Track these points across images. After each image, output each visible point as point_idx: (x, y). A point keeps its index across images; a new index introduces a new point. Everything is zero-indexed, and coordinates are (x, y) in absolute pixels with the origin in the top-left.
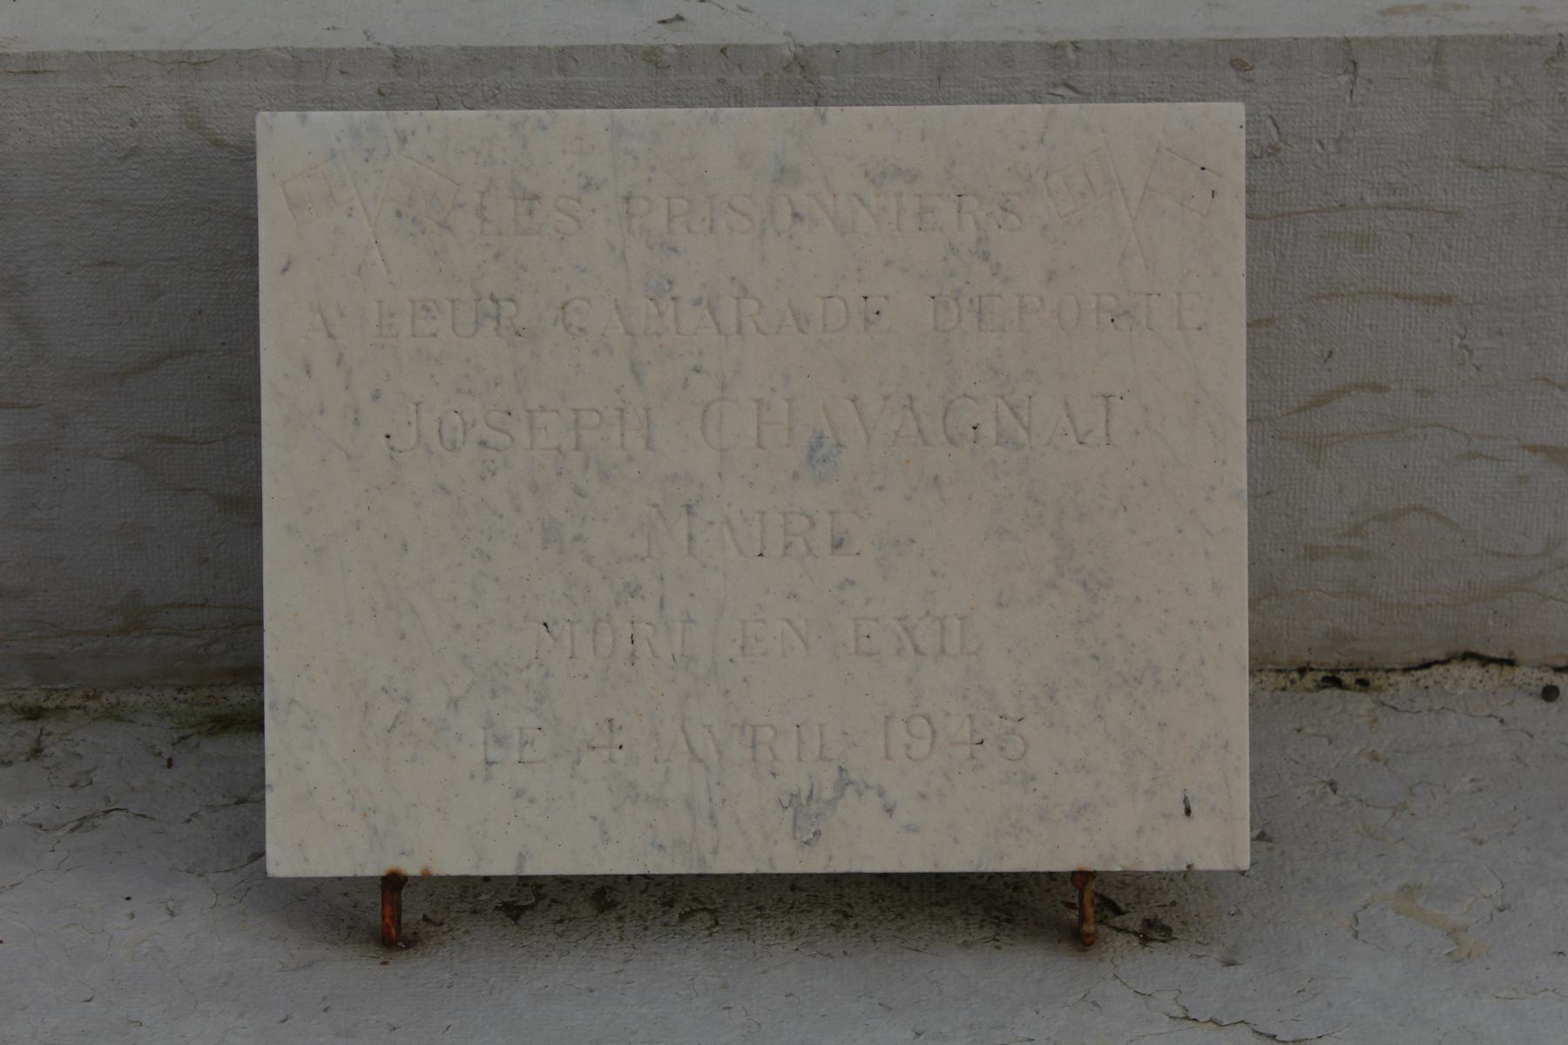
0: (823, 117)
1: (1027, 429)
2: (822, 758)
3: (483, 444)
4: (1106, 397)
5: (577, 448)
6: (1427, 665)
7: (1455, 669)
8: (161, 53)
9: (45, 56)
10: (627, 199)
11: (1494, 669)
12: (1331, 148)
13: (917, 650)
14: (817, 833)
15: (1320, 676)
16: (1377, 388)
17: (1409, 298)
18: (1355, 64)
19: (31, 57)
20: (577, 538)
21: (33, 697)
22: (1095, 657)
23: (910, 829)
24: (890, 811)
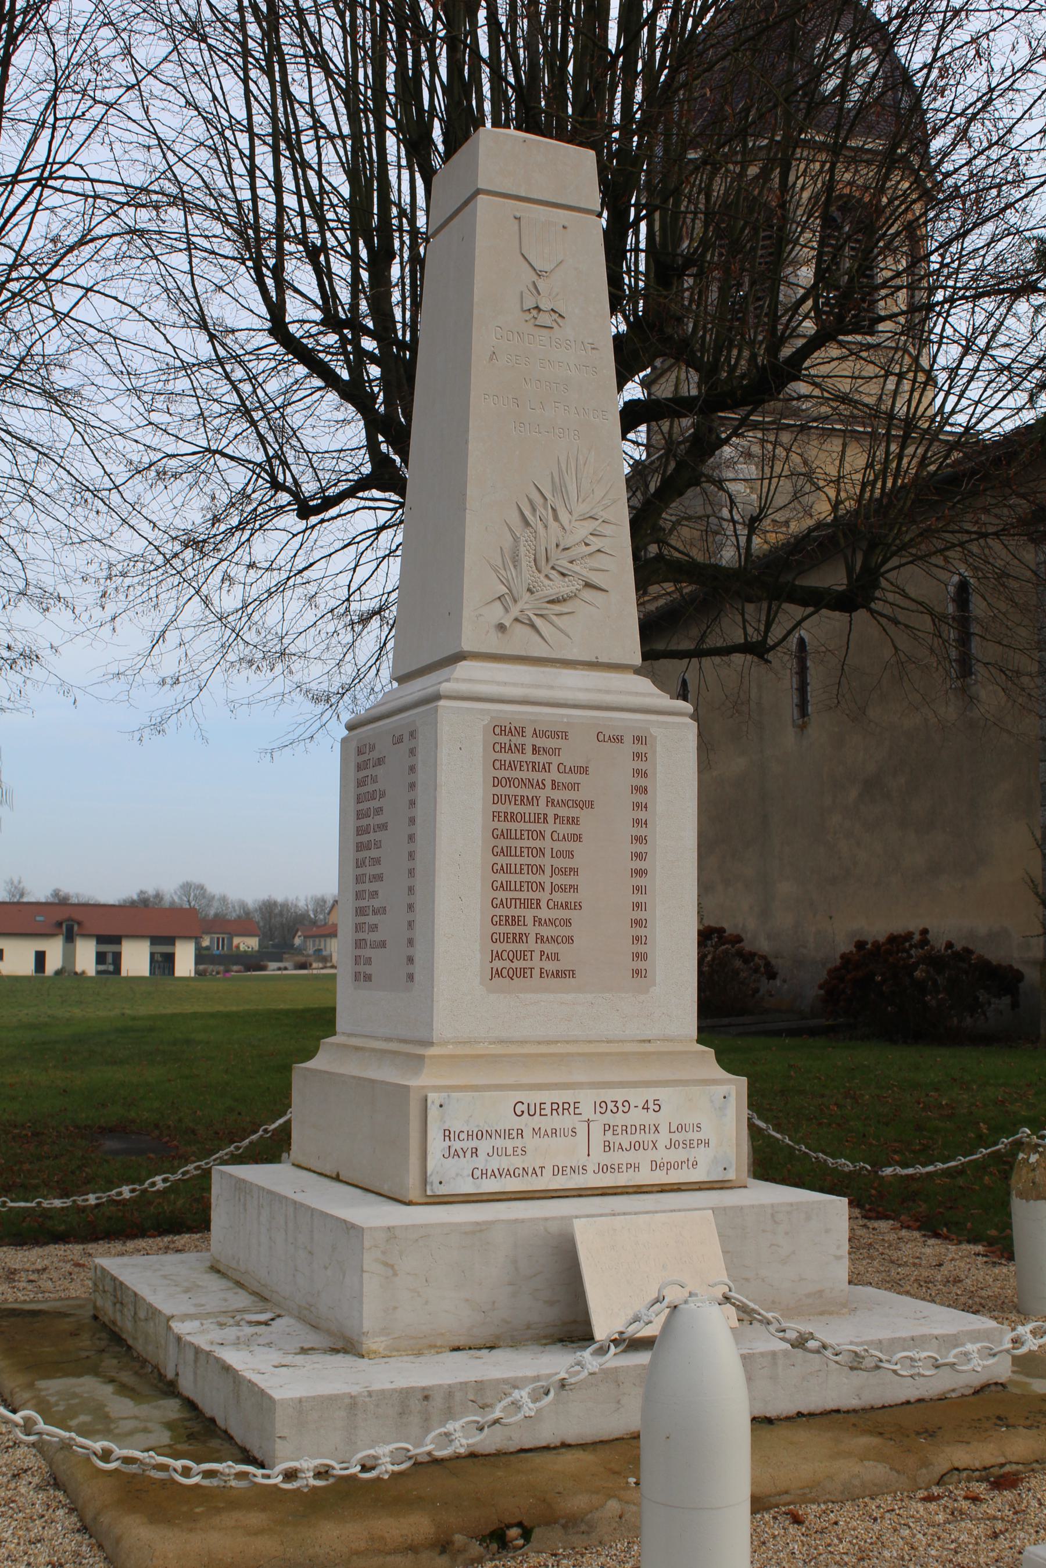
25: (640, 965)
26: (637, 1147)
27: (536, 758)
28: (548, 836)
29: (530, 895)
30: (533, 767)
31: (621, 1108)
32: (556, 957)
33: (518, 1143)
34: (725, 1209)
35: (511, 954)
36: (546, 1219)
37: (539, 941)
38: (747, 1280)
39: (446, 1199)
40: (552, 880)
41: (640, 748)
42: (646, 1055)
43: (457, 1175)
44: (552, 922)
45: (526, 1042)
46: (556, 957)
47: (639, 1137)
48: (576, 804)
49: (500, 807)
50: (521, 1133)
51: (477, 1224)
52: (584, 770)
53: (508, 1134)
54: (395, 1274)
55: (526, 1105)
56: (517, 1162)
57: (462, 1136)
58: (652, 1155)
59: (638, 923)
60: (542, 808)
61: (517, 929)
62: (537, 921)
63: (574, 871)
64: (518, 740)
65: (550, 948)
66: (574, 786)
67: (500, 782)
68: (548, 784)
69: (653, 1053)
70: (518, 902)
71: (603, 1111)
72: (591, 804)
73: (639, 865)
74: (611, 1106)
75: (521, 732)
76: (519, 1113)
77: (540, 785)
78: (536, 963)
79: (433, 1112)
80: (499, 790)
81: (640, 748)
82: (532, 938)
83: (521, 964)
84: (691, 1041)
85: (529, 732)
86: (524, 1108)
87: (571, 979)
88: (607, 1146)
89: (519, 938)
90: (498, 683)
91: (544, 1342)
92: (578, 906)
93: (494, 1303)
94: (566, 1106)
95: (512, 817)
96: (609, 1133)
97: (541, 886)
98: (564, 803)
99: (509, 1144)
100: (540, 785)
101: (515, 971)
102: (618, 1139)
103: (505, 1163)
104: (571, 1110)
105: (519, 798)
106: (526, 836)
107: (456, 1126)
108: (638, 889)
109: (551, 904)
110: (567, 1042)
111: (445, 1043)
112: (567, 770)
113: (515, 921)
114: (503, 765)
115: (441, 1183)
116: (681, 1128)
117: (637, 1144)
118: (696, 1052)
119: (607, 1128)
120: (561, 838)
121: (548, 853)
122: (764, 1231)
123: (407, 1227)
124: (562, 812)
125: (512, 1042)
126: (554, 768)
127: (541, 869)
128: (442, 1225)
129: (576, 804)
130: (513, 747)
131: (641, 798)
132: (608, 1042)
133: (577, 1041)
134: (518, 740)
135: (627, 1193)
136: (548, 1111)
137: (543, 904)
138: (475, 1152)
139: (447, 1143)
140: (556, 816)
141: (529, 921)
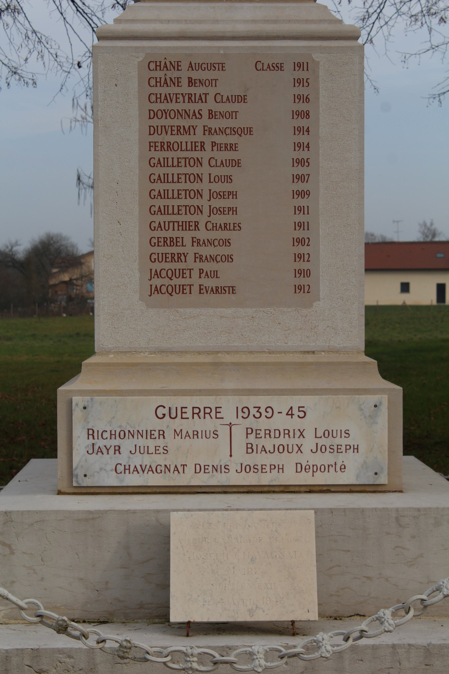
0: (253, 512)
1: (283, 556)
2: (254, 604)
3: (203, 558)
4: (295, 552)
5: (217, 559)
6: (351, 616)
7: (356, 617)
8: (153, 510)
9: (136, 510)
10: (224, 524)
11: (362, 617)
12: (330, 526)
13: (268, 588)
14: (253, 615)
15: (334, 618)
16: (339, 566)
17: (343, 551)
18: (332, 512)
19: (134, 510)
20: (217, 572)
21: (123, 620)
22: (294, 589)
23: (267, 614)
24: (264, 612)
25: (303, 281)
26: (281, 450)
27: (192, 90)
28: (205, 162)
29: (188, 218)
30: (189, 98)
31: (264, 413)
32: (215, 275)
33: (160, 442)
34: (345, 510)
35: (170, 272)
36: (158, 511)
37: (198, 260)
38: (369, 578)
39: (92, 490)
40: (210, 203)
41: (302, 74)
42: (302, 365)
43: (101, 469)
44: (211, 243)
45: (186, 352)
46: (215, 275)
47: (283, 441)
48: (234, 131)
49: (156, 138)
50: (162, 434)
51: (90, 512)
52: (243, 99)
53: (150, 434)
54: (12, 553)
55: (167, 409)
56: (160, 460)
57: (105, 435)
58: (295, 457)
59: (300, 241)
60: (199, 137)
61: (175, 250)
62: (196, 242)
63: (233, 194)
64: (173, 74)
65: (208, 267)
66: (232, 115)
67: (156, 114)
68: (205, 113)
69: (311, 364)
70: (176, 225)
71: (245, 416)
72: (250, 131)
73: (301, 186)
74: (253, 411)
75: (177, 66)
76: (161, 416)
77: (197, 115)
78: (195, 280)
79: (77, 414)
80: (156, 122)
81: (302, 74)
82: (190, 258)
83: (181, 281)
84: (358, 353)
85: (185, 65)
86: (166, 411)
87: (231, 295)
88: (250, 448)
89: (178, 257)
90: (161, 21)
91: (157, 620)
92: (237, 227)
93: (107, 583)
94: (208, 410)
95: (169, 146)
96: (252, 438)
97: (199, 209)
98: (222, 131)
99: (151, 444)
100: (197, 115)
101: (174, 288)
102: (261, 442)
103: (147, 460)
104: (213, 414)
105: (175, 129)
106: (183, 163)
107: (99, 426)
108: (300, 209)
109: (210, 226)
110: (228, 353)
111: (109, 352)
112: (224, 100)
113: (173, 242)
114: (158, 99)
115: (85, 476)
116: (328, 434)
117: (281, 448)
118: (365, 363)
119: (249, 431)
120: (219, 164)
121: (206, 178)
122: (388, 534)
123: (23, 513)
124: (220, 139)
125: (172, 352)
126: (210, 98)
127: (199, 194)
128: (57, 512)
129: (234, 131)
130: (168, 81)
131: (302, 122)
132: (270, 353)
133: (236, 352)
134: (173, 74)
135: (274, 492)
136: (189, 414)
137: (202, 226)
138: (118, 449)
139: (91, 440)
140: (214, 144)
141: (188, 241)
